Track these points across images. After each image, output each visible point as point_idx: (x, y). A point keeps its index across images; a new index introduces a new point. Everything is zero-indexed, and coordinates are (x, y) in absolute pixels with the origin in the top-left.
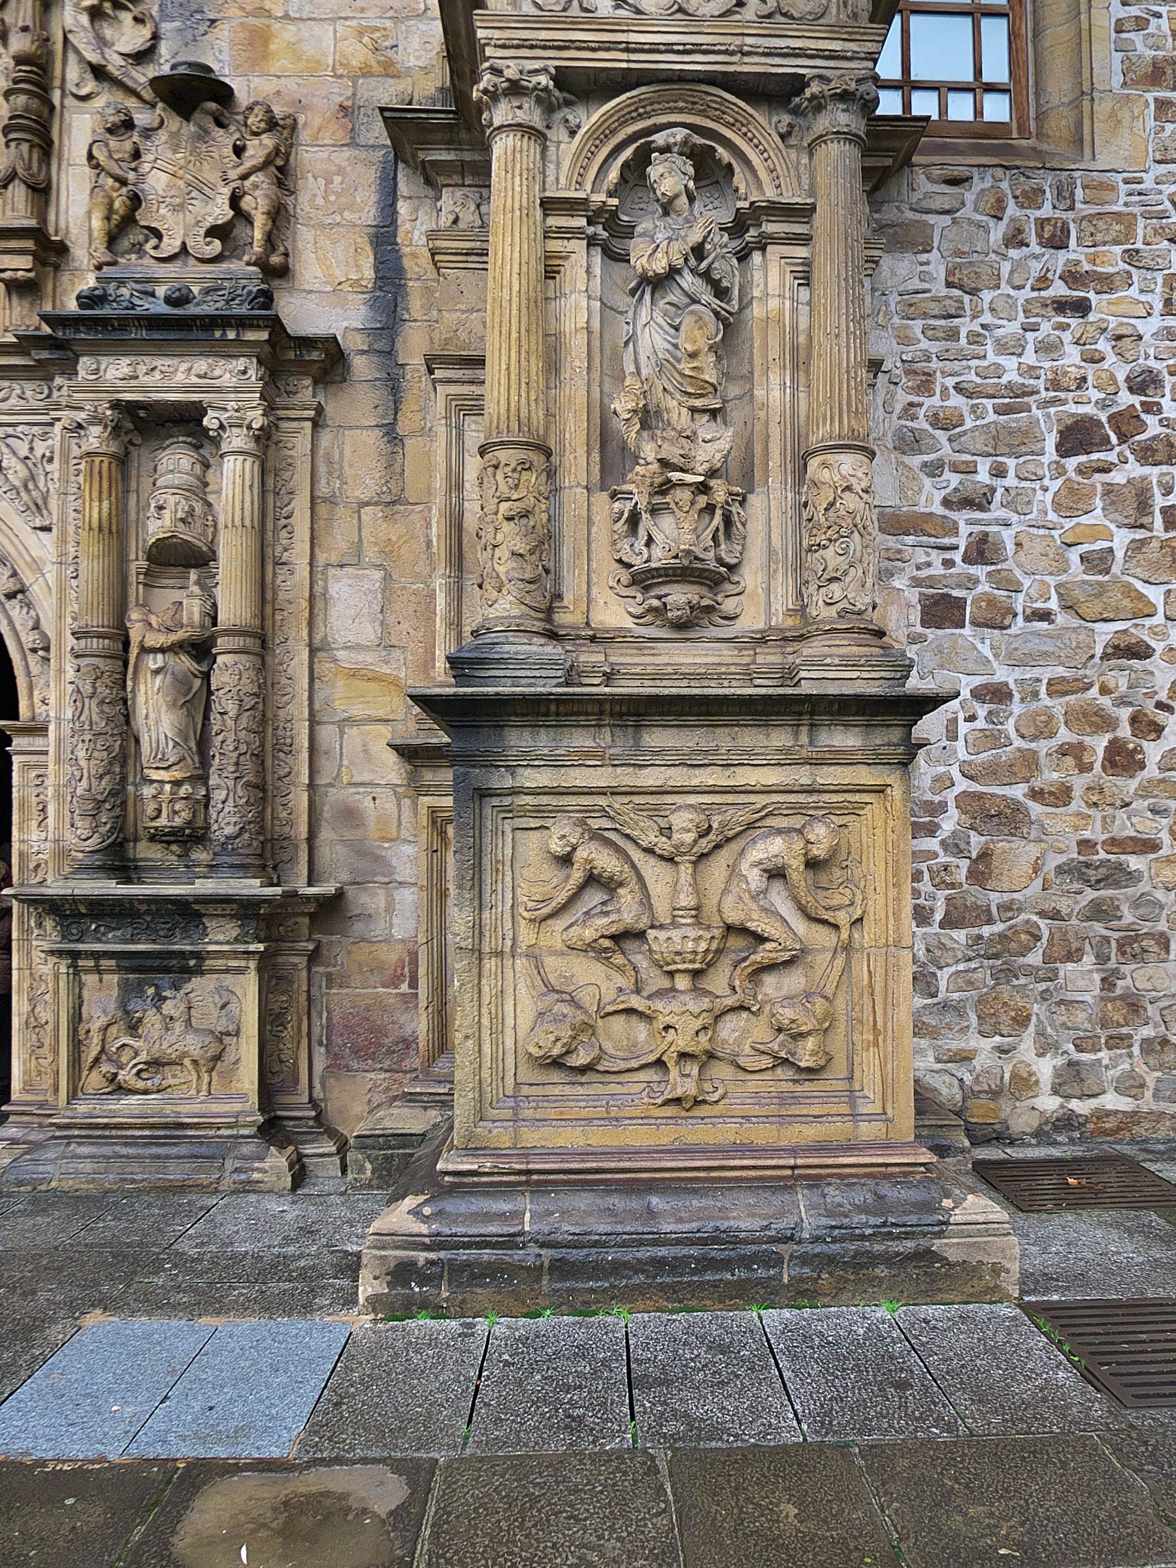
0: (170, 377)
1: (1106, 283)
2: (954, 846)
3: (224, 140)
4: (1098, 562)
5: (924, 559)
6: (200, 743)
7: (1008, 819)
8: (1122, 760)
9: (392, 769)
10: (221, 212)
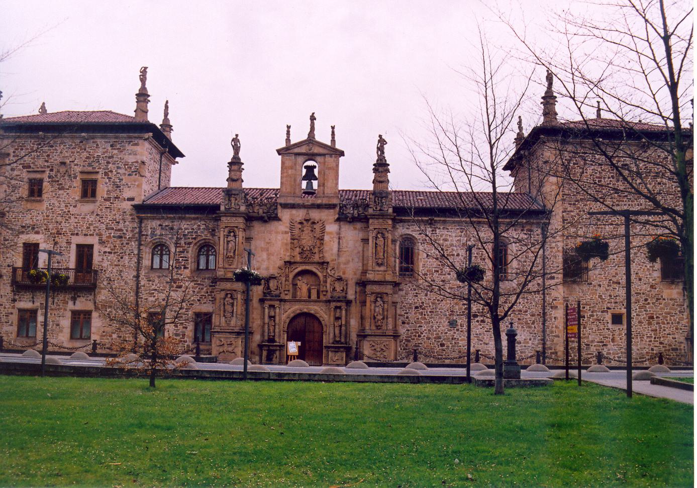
0: (339, 304)
1: (419, 294)
2: (404, 343)
3: (342, 282)
4: (418, 319)
5: (402, 318)
6: (340, 333)
7: (409, 341)
8: (419, 336)
9: (356, 336)
10: (342, 289)
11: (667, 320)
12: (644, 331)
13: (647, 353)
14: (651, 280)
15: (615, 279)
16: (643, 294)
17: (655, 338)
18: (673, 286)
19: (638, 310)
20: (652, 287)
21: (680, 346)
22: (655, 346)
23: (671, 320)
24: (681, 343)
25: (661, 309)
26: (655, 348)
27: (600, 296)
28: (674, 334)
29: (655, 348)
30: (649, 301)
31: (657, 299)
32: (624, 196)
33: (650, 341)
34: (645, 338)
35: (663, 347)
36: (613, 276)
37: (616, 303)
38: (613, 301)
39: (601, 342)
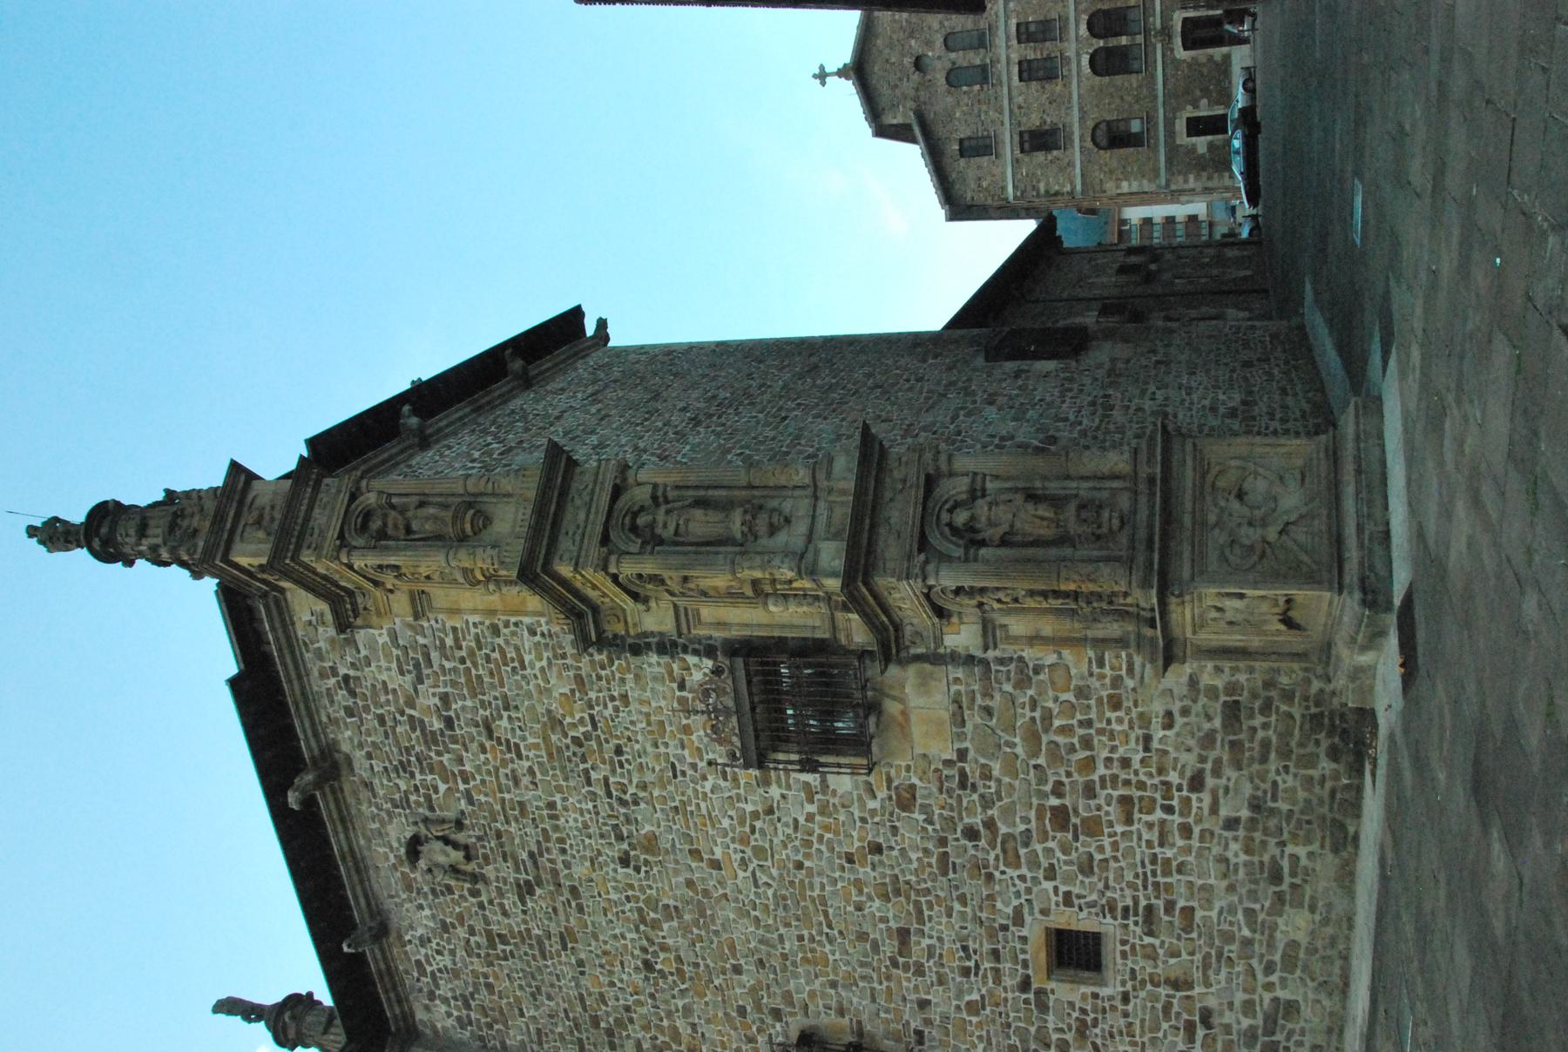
11: (1072, 749)
12: (1130, 852)
13: (1248, 850)
14: (872, 804)
15: (889, 947)
16: (943, 842)
17: (1169, 810)
18: (892, 708)
19: (1024, 871)
20: (906, 799)
21: (1212, 692)
22: (1214, 809)
23: (1064, 730)
24: (1193, 682)
25: (1011, 768)
26: (1224, 812)
27: (973, 1008)
28: (1145, 720)
29: (1224, 812)
30: (977, 820)
31: (963, 785)
32: (535, 863)
33: (1186, 831)
34: (1169, 853)
35: (1217, 772)
36: (875, 947)
37: (995, 954)
38: (987, 965)
39: (1190, 1028)
